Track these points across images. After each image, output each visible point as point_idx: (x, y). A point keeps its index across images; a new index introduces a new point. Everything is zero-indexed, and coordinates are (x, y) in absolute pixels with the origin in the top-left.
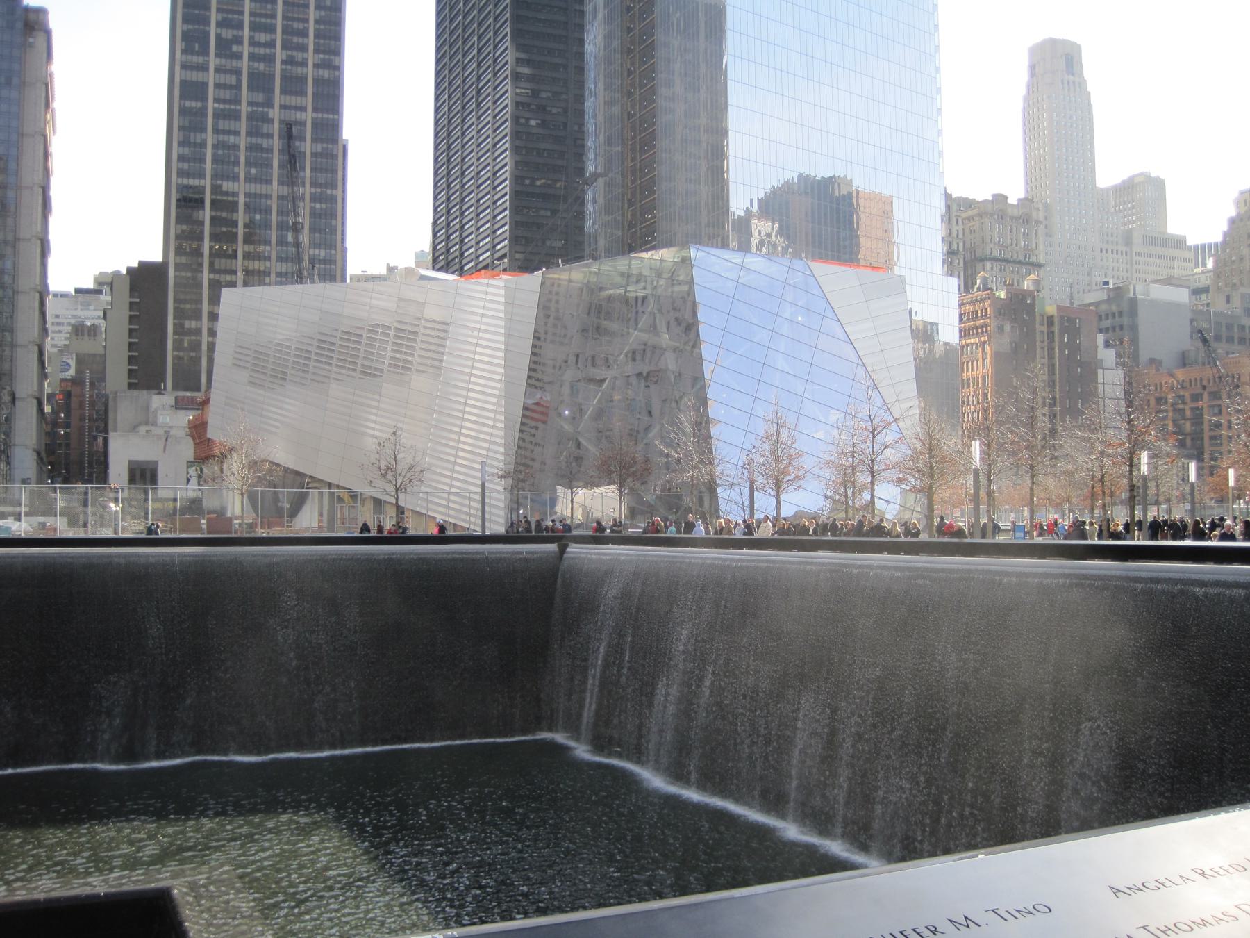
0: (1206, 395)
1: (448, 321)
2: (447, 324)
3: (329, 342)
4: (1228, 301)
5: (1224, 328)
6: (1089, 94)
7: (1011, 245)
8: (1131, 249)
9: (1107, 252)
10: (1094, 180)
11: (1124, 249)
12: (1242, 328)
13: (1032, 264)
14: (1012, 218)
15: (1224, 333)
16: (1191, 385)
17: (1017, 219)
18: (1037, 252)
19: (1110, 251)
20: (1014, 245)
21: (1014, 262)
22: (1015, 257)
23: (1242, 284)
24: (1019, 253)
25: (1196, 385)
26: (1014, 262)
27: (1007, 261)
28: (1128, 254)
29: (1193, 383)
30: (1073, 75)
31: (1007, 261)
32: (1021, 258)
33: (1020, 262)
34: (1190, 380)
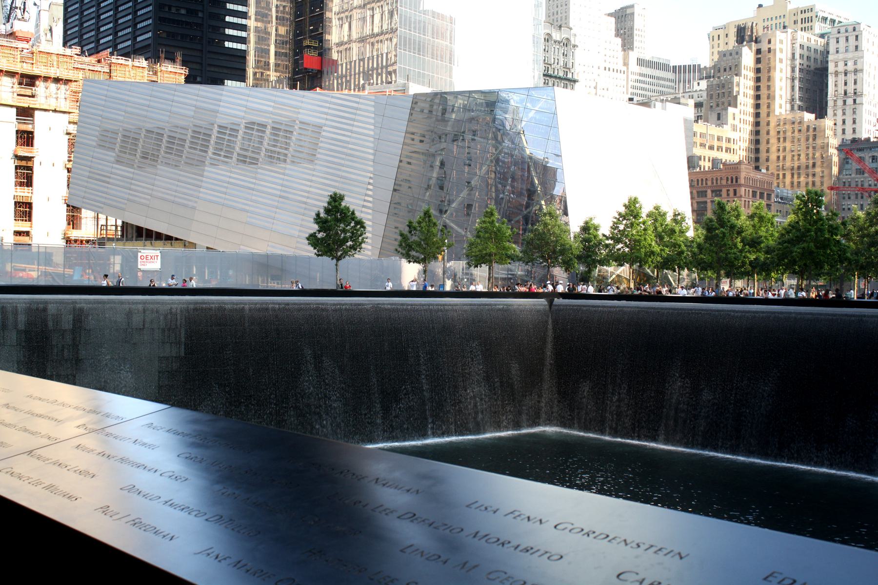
0: (709, 192)
3: (204, 134)
4: (719, 119)
5: (716, 139)
7: (554, 63)
8: (628, 68)
9: (609, 70)
11: (625, 68)
12: (729, 140)
13: (569, 80)
14: (555, 42)
15: (716, 144)
16: (698, 184)
17: (559, 42)
18: (572, 71)
20: (556, 64)
21: (556, 77)
22: (556, 73)
23: (730, 105)
24: (560, 71)
25: (702, 184)
26: (556, 77)
27: (550, 76)
28: (626, 72)
29: (700, 182)
31: (550, 76)
32: (561, 74)
33: (560, 78)
34: (698, 180)
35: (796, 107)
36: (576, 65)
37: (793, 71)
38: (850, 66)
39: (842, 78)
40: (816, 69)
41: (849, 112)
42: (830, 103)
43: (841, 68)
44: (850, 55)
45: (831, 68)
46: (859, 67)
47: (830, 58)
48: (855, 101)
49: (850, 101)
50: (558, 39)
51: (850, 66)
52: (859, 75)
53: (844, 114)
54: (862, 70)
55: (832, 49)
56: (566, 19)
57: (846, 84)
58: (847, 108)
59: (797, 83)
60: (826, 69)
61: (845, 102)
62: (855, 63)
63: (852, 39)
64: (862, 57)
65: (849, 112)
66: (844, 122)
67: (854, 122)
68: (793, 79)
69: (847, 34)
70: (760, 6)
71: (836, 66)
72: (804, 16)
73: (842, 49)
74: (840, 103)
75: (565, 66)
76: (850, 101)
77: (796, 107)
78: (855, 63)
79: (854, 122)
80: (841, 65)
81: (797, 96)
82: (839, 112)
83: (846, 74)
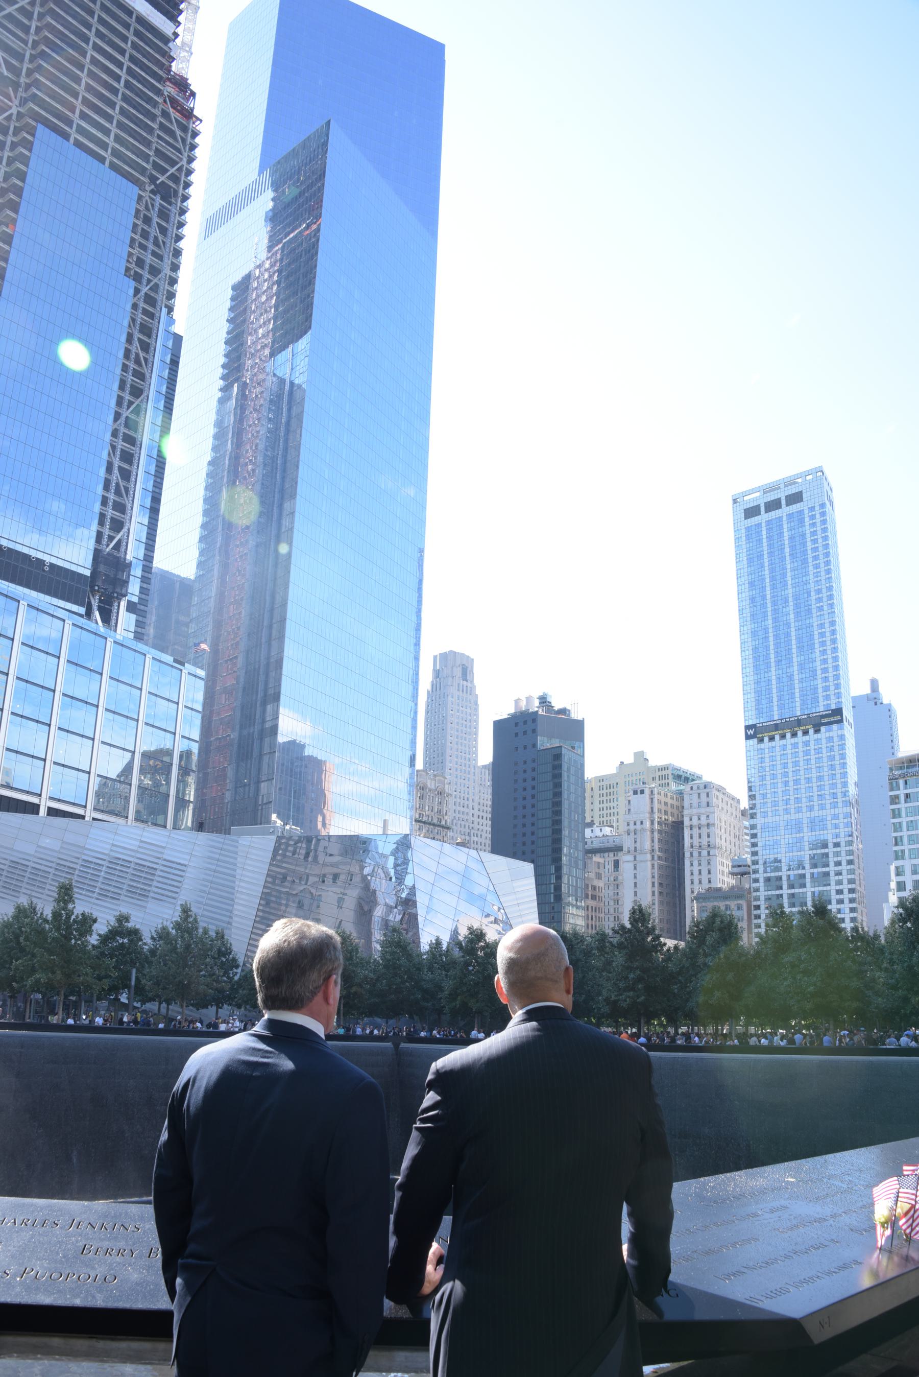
1: (185, 863)
2: (185, 865)
6: (477, 696)
10: (476, 760)
12: (594, 888)
13: (443, 827)
14: (430, 791)
19: (485, 818)
21: (430, 824)
30: (467, 681)
32: (435, 821)
33: (434, 825)
35: (656, 858)
36: (449, 813)
37: (652, 823)
38: (704, 821)
39: (696, 831)
40: (673, 822)
41: (704, 863)
42: (687, 854)
43: (695, 822)
44: (703, 810)
45: (687, 822)
46: (711, 821)
47: (685, 812)
48: (709, 852)
49: (704, 853)
50: (433, 787)
51: (704, 821)
52: (712, 828)
53: (700, 864)
54: (714, 825)
55: (686, 804)
56: (442, 769)
57: (700, 837)
58: (702, 859)
59: (656, 835)
60: (682, 823)
61: (700, 853)
62: (708, 816)
63: (703, 796)
64: (714, 813)
65: (704, 863)
66: (700, 873)
67: (709, 873)
68: (652, 831)
69: (699, 791)
70: (622, 763)
71: (691, 820)
72: (661, 773)
73: (695, 805)
74: (695, 854)
75: (439, 812)
76: (704, 853)
77: (656, 858)
78: (708, 816)
79: (709, 873)
80: (695, 819)
81: (656, 847)
82: (696, 863)
83: (700, 828)
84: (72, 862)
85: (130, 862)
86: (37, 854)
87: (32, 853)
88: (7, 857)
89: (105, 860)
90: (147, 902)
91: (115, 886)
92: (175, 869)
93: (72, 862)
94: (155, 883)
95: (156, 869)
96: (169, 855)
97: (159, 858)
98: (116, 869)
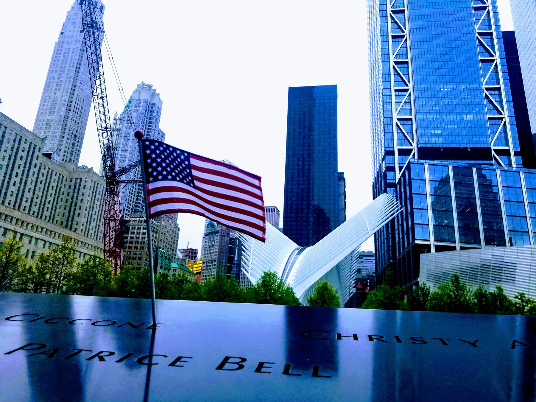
2: (515, 264)
84: (466, 269)
85: (490, 266)
86: (452, 268)
87: (450, 268)
88: (441, 271)
89: (478, 266)
90: (502, 284)
91: (486, 278)
92: (511, 266)
93: (466, 269)
94: (503, 274)
95: (502, 267)
96: (506, 259)
97: (502, 262)
98: (485, 270)
